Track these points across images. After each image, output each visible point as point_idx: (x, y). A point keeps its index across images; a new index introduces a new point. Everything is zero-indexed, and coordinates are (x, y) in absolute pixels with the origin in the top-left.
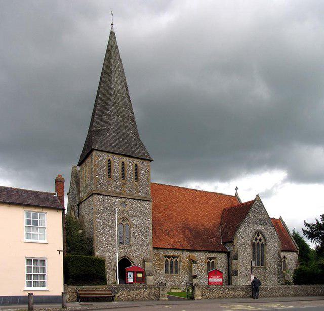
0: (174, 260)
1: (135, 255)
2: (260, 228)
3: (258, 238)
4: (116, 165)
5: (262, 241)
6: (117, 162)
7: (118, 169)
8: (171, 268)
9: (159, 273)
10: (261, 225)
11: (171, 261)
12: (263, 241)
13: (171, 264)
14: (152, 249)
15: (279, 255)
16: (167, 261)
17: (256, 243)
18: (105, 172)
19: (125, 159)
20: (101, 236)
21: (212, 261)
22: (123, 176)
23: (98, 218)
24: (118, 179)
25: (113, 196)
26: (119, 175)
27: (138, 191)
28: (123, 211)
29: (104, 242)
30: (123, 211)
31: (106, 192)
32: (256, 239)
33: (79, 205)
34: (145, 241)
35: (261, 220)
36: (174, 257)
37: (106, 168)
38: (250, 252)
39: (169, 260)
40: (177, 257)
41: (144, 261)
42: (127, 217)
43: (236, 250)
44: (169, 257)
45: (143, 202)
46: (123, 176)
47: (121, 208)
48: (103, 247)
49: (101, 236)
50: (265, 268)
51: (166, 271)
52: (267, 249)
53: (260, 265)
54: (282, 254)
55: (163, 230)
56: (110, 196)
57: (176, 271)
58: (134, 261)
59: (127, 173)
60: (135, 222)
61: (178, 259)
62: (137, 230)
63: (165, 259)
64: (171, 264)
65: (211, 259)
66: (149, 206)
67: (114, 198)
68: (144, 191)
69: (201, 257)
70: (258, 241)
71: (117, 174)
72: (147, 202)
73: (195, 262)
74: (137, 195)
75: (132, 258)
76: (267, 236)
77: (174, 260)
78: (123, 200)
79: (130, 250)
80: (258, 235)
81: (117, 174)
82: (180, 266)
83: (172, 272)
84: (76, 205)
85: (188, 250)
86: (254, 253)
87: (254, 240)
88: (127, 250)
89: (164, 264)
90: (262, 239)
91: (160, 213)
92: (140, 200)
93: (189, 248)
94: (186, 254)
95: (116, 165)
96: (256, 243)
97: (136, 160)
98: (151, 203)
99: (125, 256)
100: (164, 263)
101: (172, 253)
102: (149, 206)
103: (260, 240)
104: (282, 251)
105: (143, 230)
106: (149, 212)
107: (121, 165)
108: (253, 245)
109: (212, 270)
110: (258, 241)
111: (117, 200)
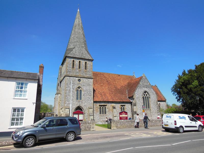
1: (85, 105)
7: (77, 64)
9: (97, 114)
13: (103, 110)
15: (157, 103)
16: (100, 108)
18: (71, 66)
20: (68, 96)
22: (79, 67)
23: (67, 87)
24: (77, 69)
25: (74, 77)
26: (78, 67)
27: (86, 74)
32: (144, 95)
33: (61, 82)
34: (89, 98)
35: (146, 86)
36: (104, 106)
37: (72, 64)
38: (142, 101)
40: (106, 105)
42: (81, 86)
44: (102, 106)
45: (89, 79)
46: (79, 67)
47: (78, 82)
49: (68, 96)
50: (150, 110)
51: (100, 113)
52: (150, 100)
53: (148, 108)
54: (159, 103)
56: (73, 77)
57: (105, 113)
58: (84, 108)
59: (81, 66)
62: (86, 92)
64: (103, 110)
65: (123, 106)
68: (90, 74)
70: (145, 96)
72: (91, 79)
74: (86, 76)
75: (83, 107)
76: (150, 93)
78: (79, 78)
79: (82, 103)
80: (145, 93)
82: (107, 110)
83: (103, 113)
84: (59, 83)
86: (144, 102)
88: (80, 103)
89: (99, 109)
91: (98, 85)
92: (88, 78)
93: (111, 101)
98: (92, 79)
99: (79, 106)
104: (159, 101)
107: (79, 63)
108: (143, 98)
110: (145, 96)
111: (76, 78)
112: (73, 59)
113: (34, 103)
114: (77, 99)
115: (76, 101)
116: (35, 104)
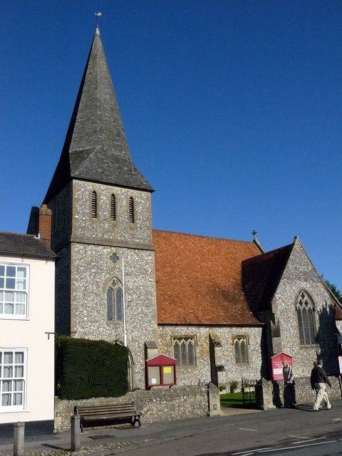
0: (187, 343)
2: (305, 285)
3: (304, 301)
4: (104, 200)
5: (309, 305)
6: (105, 192)
7: (106, 204)
8: (184, 356)
10: (305, 281)
11: (184, 345)
12: (310, 305)
14: (156, 326)
16: (177, 345)
17: (301, 308)
19: (116, 190)
20: (81, 309)
21: (241, 340)
28: (114, 268)
29: (85, 318)
30: (114, 268)
31: (88, 239)
32: (301, 303)
34: (146, 315)
38: (295, 323)
39: (180, 343)
41: (146, 348)
43: (276, 321)
44: (180, 339)
47: (110, 263)
48: (83, 328)
49: (81, 309)
55: (166, 297)
60: (130, 285)
61: (193, 342)
62: (135, 296)
63: (174, 342)
65: (239, 337)
66: (149, 257)
67: (100, 248)
69: (224, 334)
70: (304, 305)
71: (104, 211)
72: (148, 252)
73: (219, 344)
76: (315, 298)
77: (187, 343)
80: (303, 296)
81: (104, 211)
85: (206, 326)
86: (300, 325)
87: (298, 305)
88: (119, 330)
90: (309, 301)
94: (204, 331)
95: (104, 200)
96: (301, 308)
97: (131, 191)
98: (153, 253)
100: (173, 347)
101: (184, 331)
102: (149, 257)
103: (306, 303)
105: (142, 297)
106: (150, 268)
108: (298, 311)
109: (241, 353)
110: (304, 305)
111: (105, 250)
112: (90, 186)
113: (49, 333)
114: (110, 319)
115: (107, 324)
116: (52, 337)
